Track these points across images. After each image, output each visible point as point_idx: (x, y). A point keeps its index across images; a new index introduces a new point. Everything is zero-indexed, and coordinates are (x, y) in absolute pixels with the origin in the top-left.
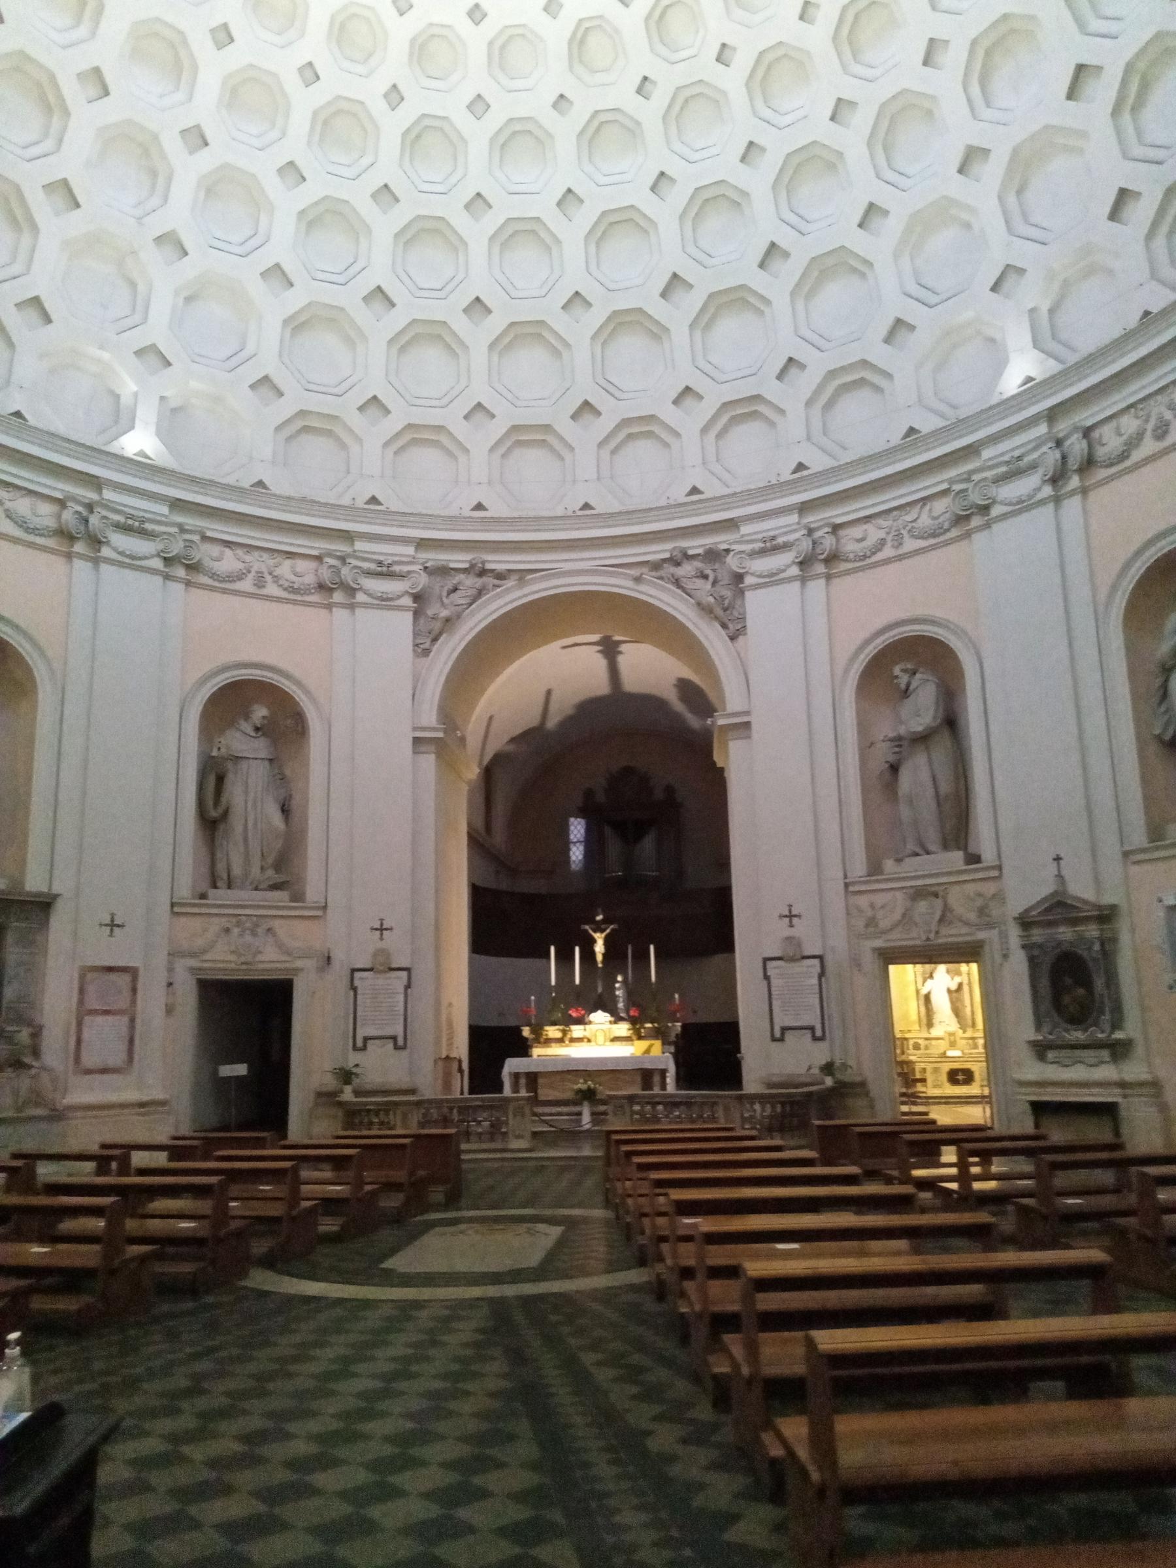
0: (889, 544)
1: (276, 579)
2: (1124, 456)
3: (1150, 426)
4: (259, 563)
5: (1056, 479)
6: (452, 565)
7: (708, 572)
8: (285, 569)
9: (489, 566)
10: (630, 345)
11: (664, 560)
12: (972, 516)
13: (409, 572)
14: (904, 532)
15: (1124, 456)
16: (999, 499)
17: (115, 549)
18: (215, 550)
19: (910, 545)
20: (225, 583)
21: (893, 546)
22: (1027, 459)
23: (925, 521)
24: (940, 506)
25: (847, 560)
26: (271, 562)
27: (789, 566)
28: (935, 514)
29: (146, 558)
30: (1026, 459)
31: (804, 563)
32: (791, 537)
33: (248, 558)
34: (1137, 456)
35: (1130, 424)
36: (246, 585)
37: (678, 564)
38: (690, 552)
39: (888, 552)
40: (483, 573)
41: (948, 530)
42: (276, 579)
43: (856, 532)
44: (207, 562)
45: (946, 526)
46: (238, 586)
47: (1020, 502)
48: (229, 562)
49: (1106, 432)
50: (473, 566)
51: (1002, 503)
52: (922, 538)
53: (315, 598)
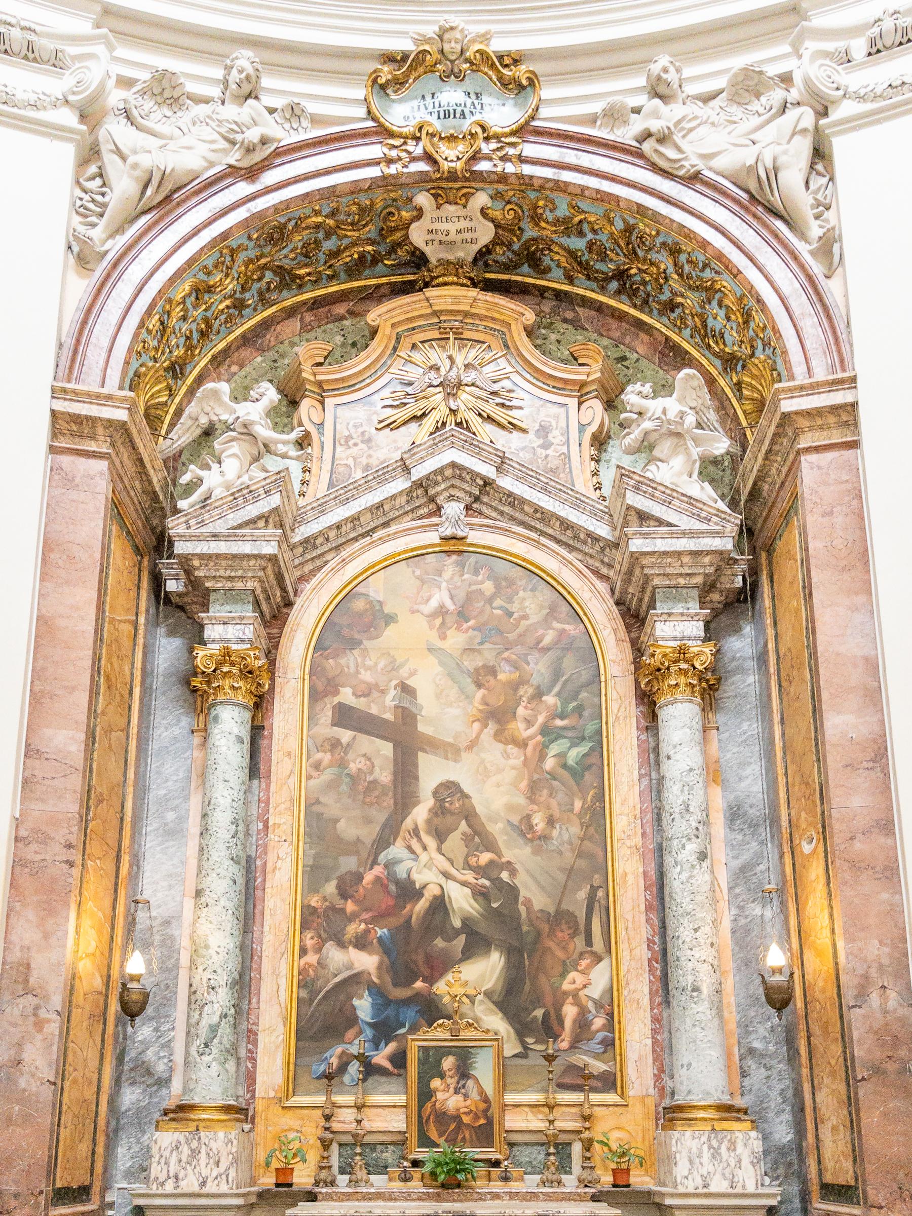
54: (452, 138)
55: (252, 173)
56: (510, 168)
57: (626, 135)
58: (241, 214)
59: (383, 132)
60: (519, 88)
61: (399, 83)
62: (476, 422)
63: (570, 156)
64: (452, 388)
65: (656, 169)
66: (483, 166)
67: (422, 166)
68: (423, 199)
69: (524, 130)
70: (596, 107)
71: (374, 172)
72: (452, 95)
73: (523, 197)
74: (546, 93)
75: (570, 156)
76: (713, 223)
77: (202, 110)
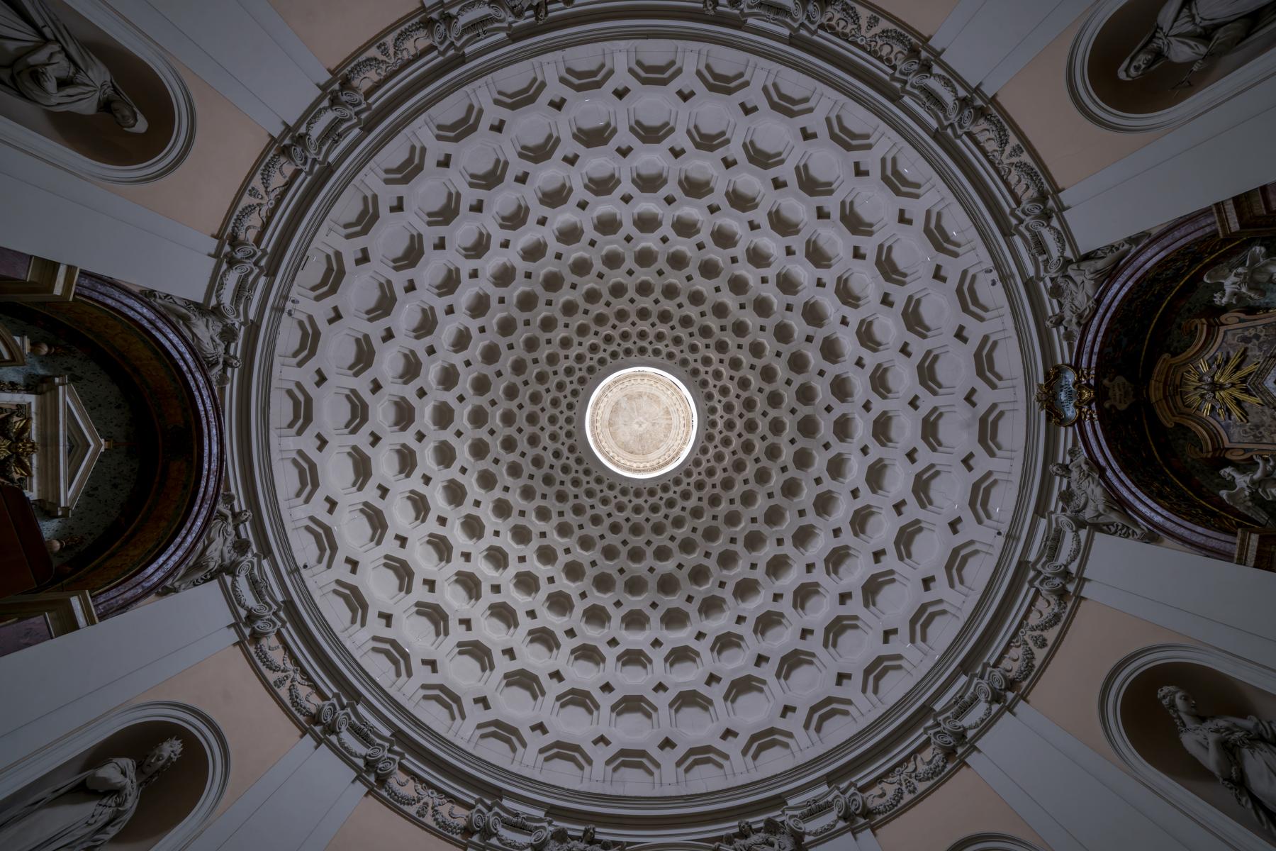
0: (906, 791)
1: (436, 812)
2: (1030, 667)
3: (1031, 644)
4: (430, 797)
5: (996, 697)
6: (570, 833)
7: (772, 839)
8: (445, 809)
9: (597, 837)
10: (689, 713)
11: (735, 835)
12: (957, 750)
13: (537, 828)
14: (913, 780)
15: (1030, 667)
16: (966, 725)
17: (339, 740)
18: (402, 777)
19: (921, 787)
20: (396, 804)
21: (910, 792)
22: (966, 698)
23: (922, 768)
24: (927, 754)
25: (880, 813)
26: (437, 801)
27: (836, 822)
28: (927, 759)
29: (356, 756)
30: (966, 698)
31: (847, 816)
32: (830, 798)
33: (422, 792)
34: (1037, 663)
35: (1016, 652)
36: (412, 810)
37: (746, 837)
38: (754, 827)
39: (908, 797)
40: (592, 841)
41: (944, 767)
42: (436, 812)
43: (876, 791)
44: (392, 782)
45: (941, 764)
46: (406, 808)
47: (982, 721)
48: (409, 789)
49: (1006, 664)
50: (586, 832)
51: (970, 728)
52: (928, 779)
53: (458, 837)
54: (1081, 395)
55: (1102, 472)
56: (1093, 372)
57: (1077, 331)
58: (1122, 475)
59: (1079, 421)
60: (1059, 371)
61: (1058, 415)
62: (1239, 374)
63: (1087, 349)
64: (1216, 387)
65: (1093, 316)
66: (1092, 382)
67: (1093, 405)
68: (1107, 405)
69: (1076, 368)
70: (1065, 344)
71: (1097, 423)
72: (1063, 396)
73: (1106, 365)
74: (1060, 362)
75: (1087, 349)
76: (1119, 290)
77: (1074, 486)
